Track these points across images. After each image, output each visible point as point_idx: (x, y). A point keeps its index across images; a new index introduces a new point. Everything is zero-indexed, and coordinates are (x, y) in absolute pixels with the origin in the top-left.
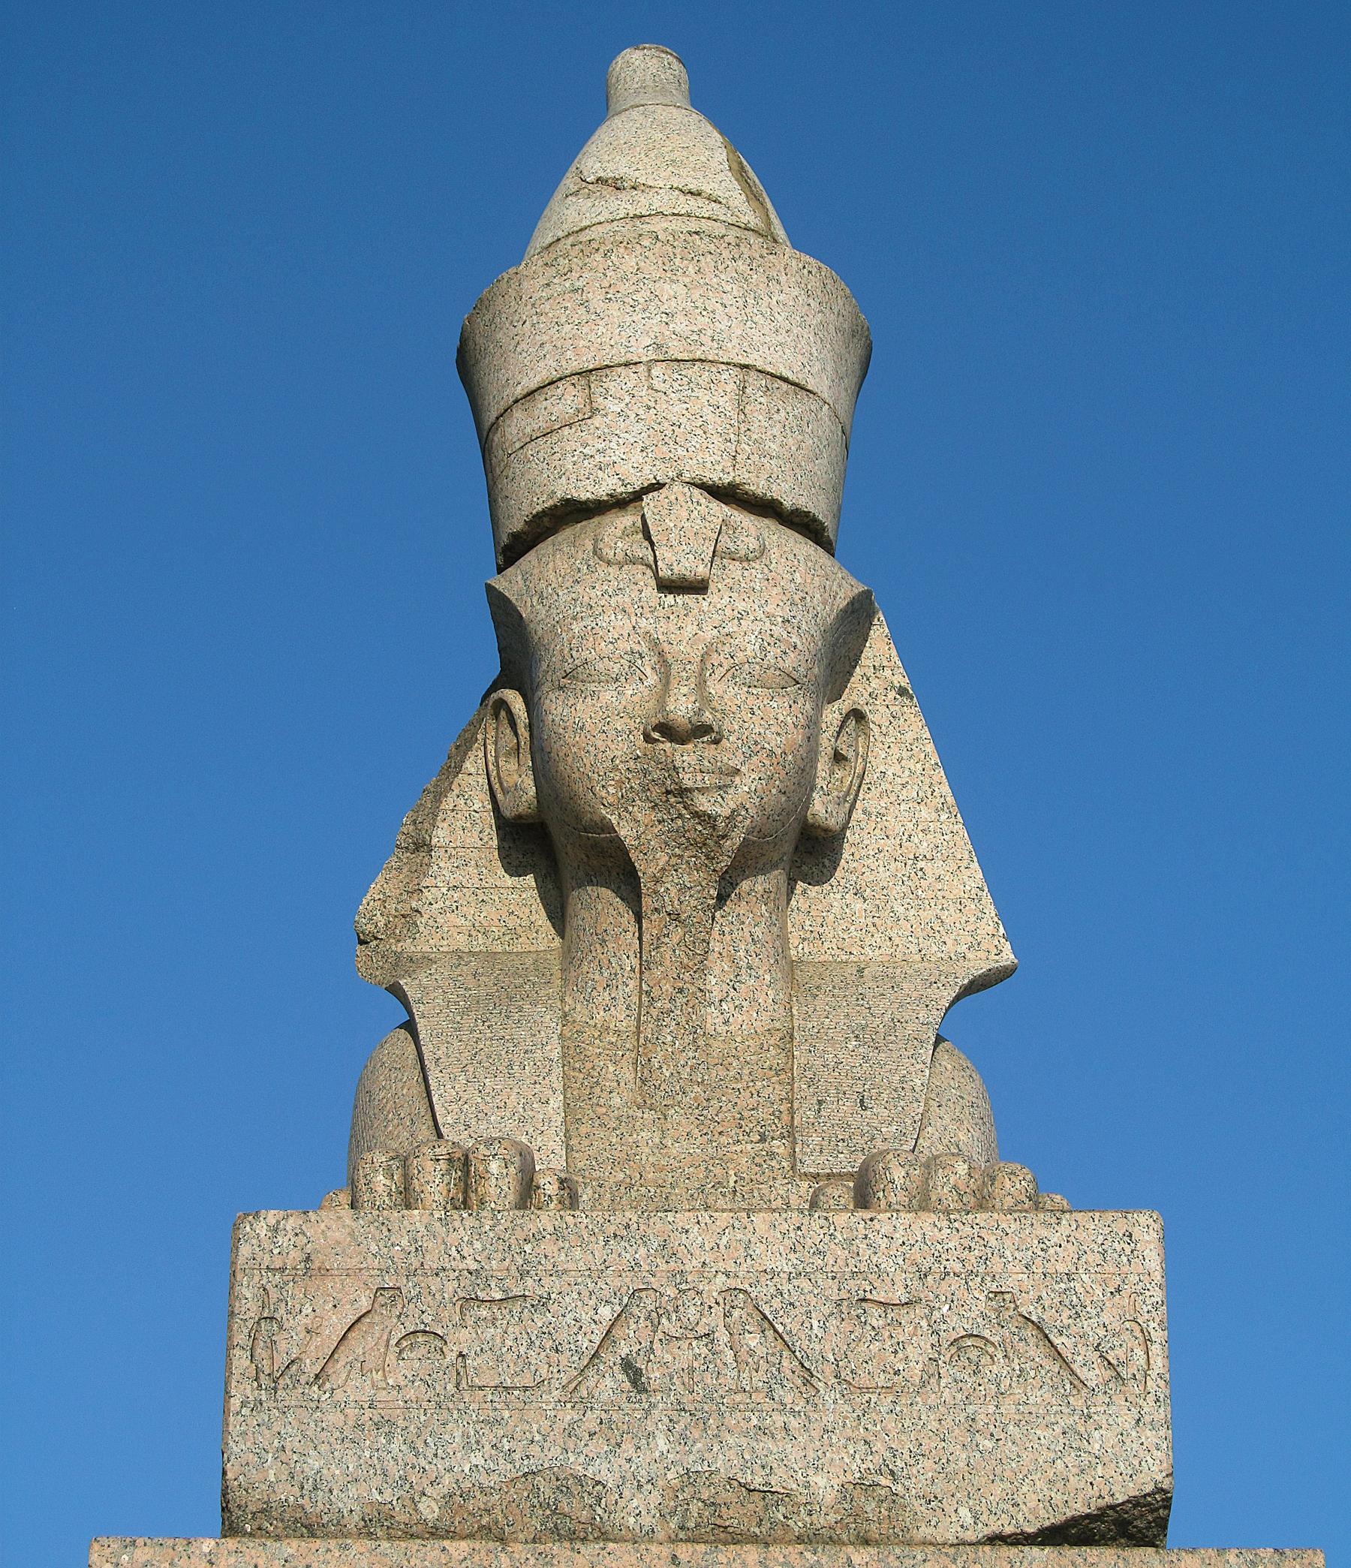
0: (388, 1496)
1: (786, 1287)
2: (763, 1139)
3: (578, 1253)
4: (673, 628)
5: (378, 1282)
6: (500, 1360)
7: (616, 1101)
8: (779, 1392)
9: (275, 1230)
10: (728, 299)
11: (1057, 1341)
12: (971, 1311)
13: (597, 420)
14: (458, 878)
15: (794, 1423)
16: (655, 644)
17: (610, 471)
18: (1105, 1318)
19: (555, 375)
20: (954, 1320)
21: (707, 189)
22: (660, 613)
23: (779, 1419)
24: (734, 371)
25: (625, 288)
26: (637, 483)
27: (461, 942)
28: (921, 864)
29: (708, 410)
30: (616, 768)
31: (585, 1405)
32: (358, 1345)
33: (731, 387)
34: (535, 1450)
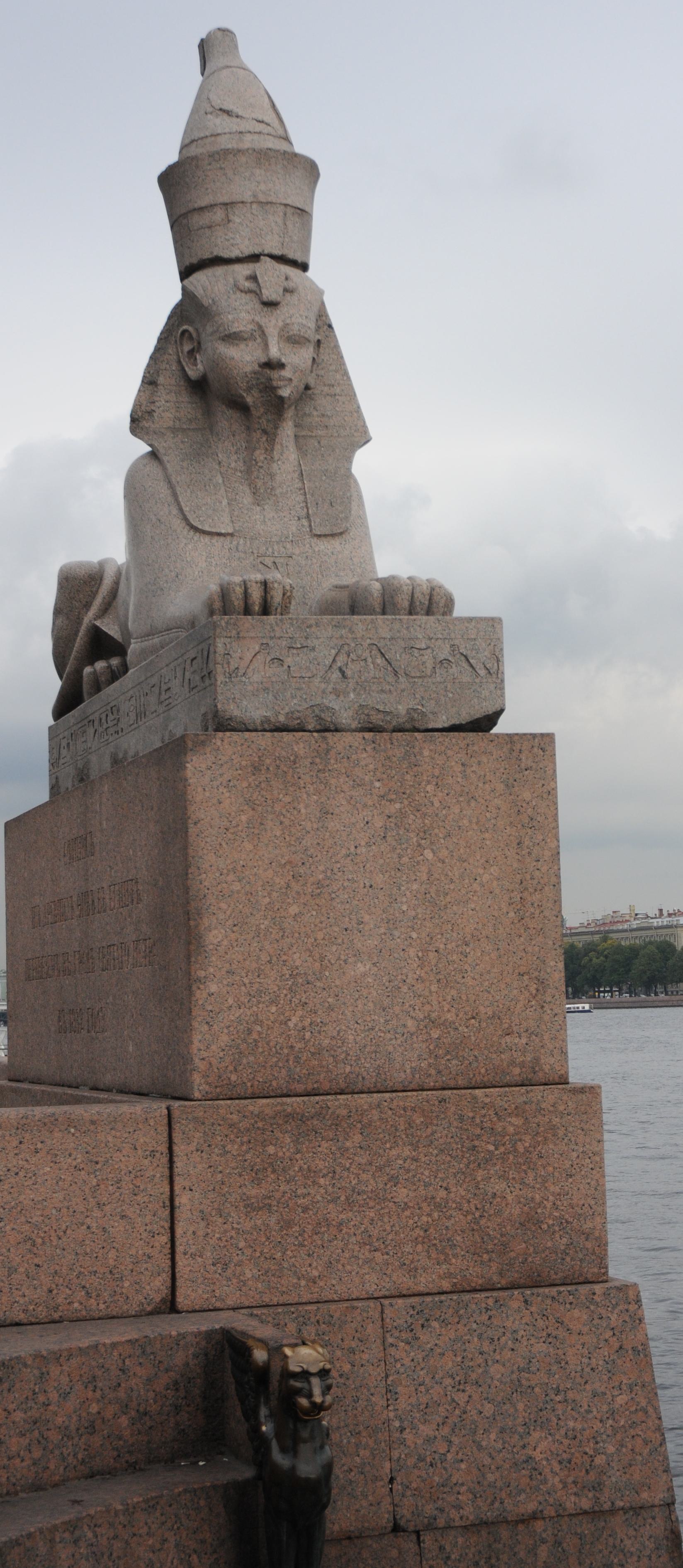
0: (268, 714)
1: (388, 643)
2: (299, 519)
4: (267, 321)
5: (261, 641)
7: (245, 502)
8: (387, 678)
9: (227, 623)
11: (472, 661)
12: (444, 652)
13: (231, 225)
14: (168, 397)
16: (260, 327)
18: (486, 653)
19: (213, 203)
20: (440, 655)
21: (266, 119)
22: (262, 314)
23: (388, 687)
24: (282, 207)
26: (247, 252)
29: (273, 224)
30: (247, 376)
31: (328, 682)
32: (255, 664)
33: (281, 214)
34: (313, 698)
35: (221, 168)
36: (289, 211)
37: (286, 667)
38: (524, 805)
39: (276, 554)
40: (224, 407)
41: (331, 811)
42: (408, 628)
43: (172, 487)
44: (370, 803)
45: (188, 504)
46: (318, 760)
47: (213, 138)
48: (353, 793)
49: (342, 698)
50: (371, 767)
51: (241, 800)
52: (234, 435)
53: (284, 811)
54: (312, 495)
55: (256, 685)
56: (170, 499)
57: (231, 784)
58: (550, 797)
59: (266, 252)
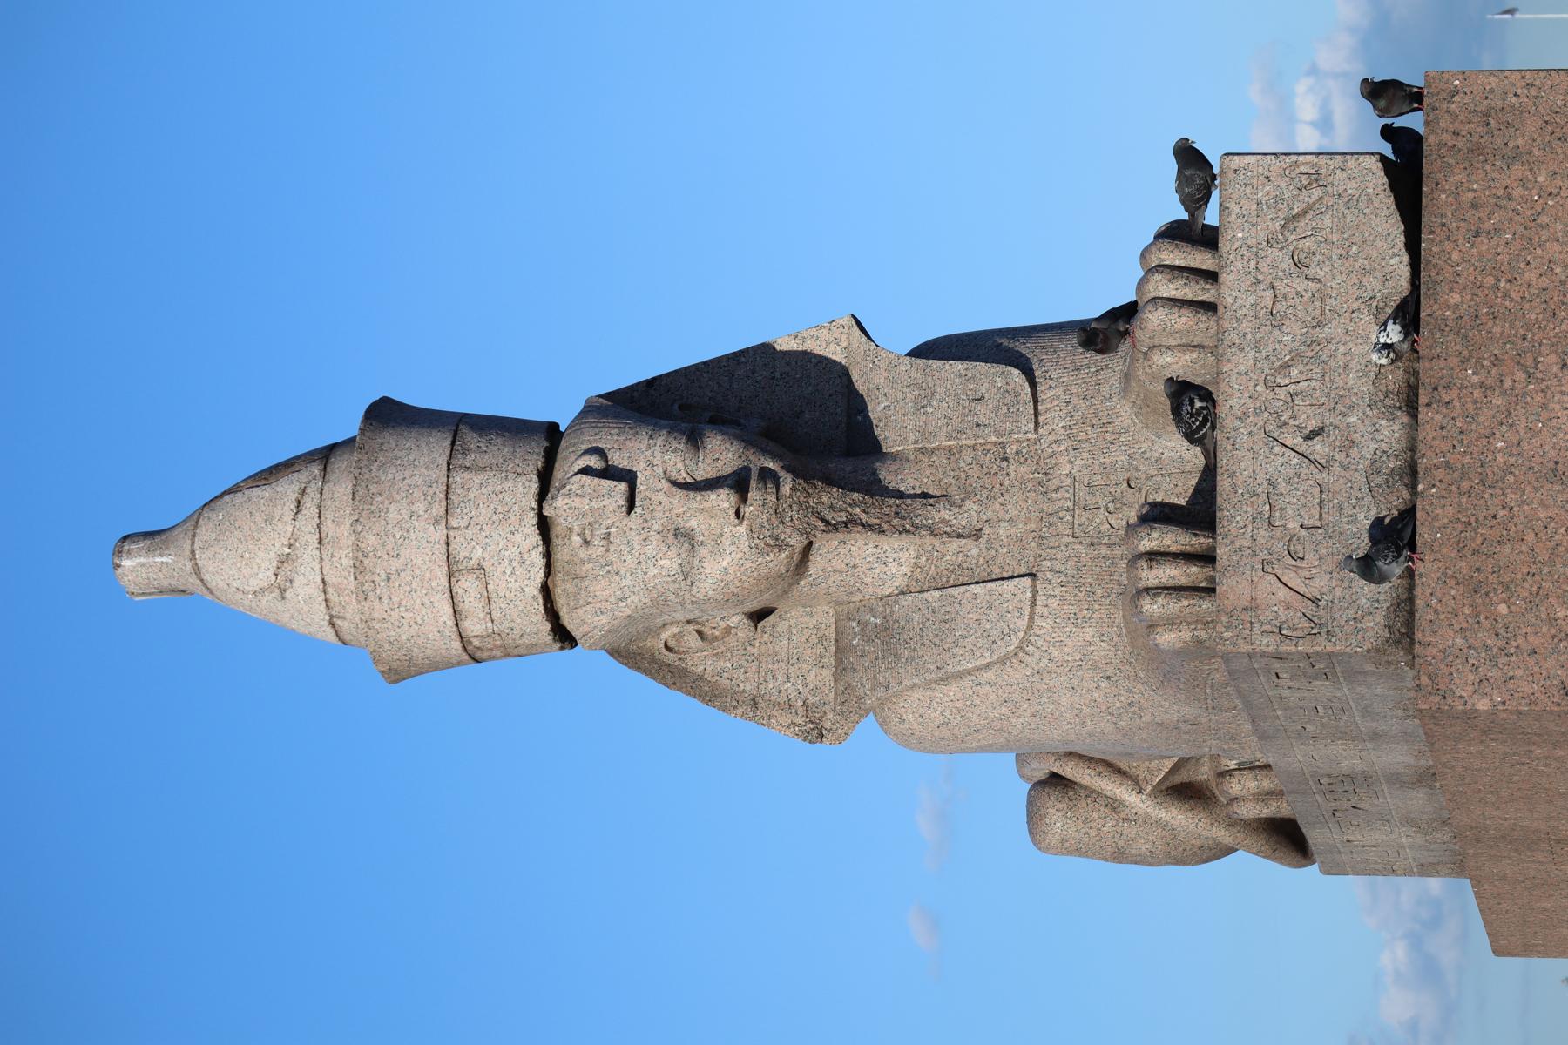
2: (1006, 459)
3: (1243, 465)
6: (1304, 506)
7: (975, 552)
8: (1324, 357)
9: (1227, 629)
10: (399, 476)
11: (1296, 211)
13: (486, 565)
15: (1342, 350)
17: (525, 556)
18: (1283, 185)
19: (448, 594)
20: (1284, 266)
25: (390, 543)
27: (827, 674)
28: (777, 375)
29: (484, 490)
35: (388, 579)
36: (459, 460)
37: (1303, 532)
38: (1549, 130)
39: (1070, 504)
40: (802, 583)
41: (1551, 464)
42: (1238, 319)
43: (947, 679)
44: (1539, 398)
45: (978, 653)
46: (1465, 485)
47: (330, 590)
48: (1522, 426)
49: (1356, 437)
50: (1477, 394)
51: (1529, 616)
52: (855, 567)
53: (1550, 545)
54: (962, 432)
55: (1334, 583)
56: (967, 682)
57: (1502, 632)
58: (1537, 83)
59: (534, 505)
